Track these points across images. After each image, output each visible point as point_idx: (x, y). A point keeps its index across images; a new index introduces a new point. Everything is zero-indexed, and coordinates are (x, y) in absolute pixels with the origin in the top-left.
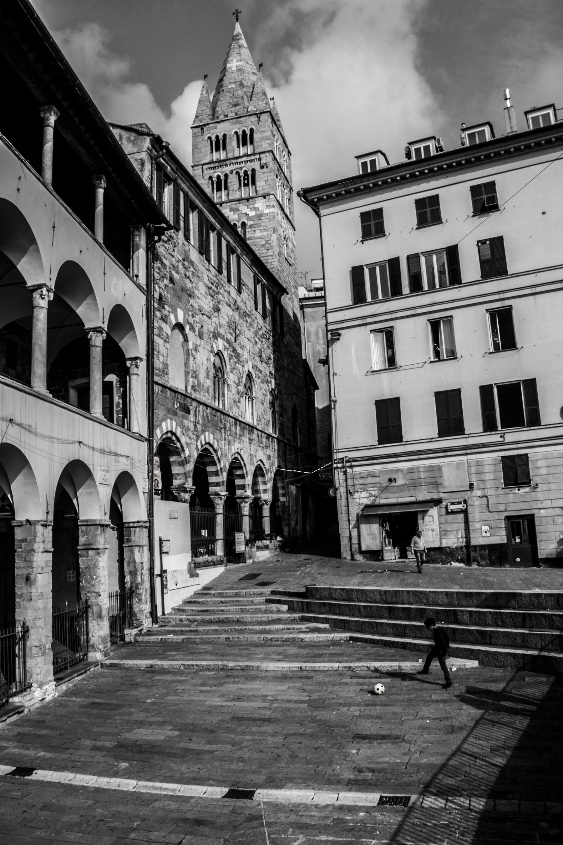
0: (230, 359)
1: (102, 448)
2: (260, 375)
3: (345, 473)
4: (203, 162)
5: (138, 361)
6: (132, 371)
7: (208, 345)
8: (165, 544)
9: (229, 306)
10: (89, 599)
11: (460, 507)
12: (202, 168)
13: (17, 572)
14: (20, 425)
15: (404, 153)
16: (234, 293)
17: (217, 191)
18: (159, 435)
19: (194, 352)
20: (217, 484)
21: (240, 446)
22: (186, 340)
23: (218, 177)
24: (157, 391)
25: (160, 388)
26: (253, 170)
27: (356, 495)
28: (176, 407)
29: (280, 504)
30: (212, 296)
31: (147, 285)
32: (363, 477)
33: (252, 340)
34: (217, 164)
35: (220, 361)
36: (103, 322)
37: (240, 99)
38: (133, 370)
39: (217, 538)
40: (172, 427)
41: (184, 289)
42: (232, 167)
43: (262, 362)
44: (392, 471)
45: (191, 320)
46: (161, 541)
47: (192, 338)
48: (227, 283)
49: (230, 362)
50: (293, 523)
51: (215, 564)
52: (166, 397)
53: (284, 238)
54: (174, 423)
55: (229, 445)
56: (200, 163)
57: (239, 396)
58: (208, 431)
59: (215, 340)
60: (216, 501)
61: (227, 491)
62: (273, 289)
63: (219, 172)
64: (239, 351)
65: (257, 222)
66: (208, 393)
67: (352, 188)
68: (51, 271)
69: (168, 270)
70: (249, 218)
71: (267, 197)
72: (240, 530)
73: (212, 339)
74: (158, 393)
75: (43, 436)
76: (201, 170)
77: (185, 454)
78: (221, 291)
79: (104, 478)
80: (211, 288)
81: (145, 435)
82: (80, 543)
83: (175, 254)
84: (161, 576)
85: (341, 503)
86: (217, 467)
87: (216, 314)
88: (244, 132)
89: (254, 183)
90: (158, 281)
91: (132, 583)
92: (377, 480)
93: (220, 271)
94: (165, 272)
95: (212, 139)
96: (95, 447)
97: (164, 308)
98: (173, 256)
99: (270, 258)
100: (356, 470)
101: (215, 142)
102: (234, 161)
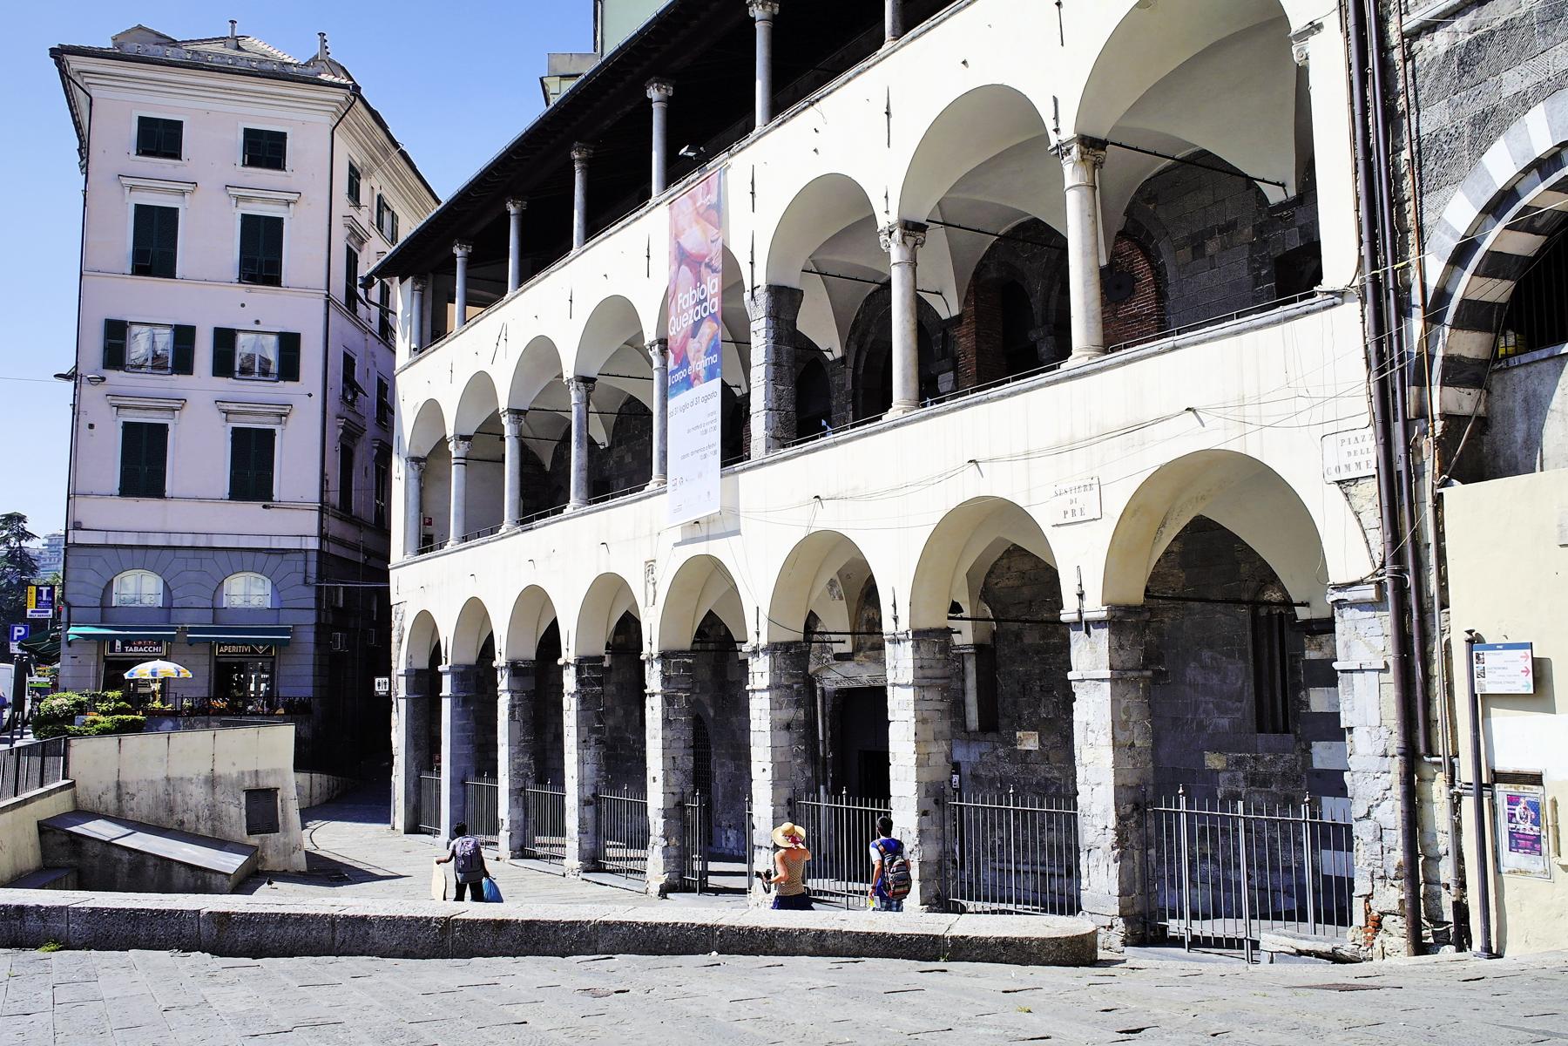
8: (1490, 658)
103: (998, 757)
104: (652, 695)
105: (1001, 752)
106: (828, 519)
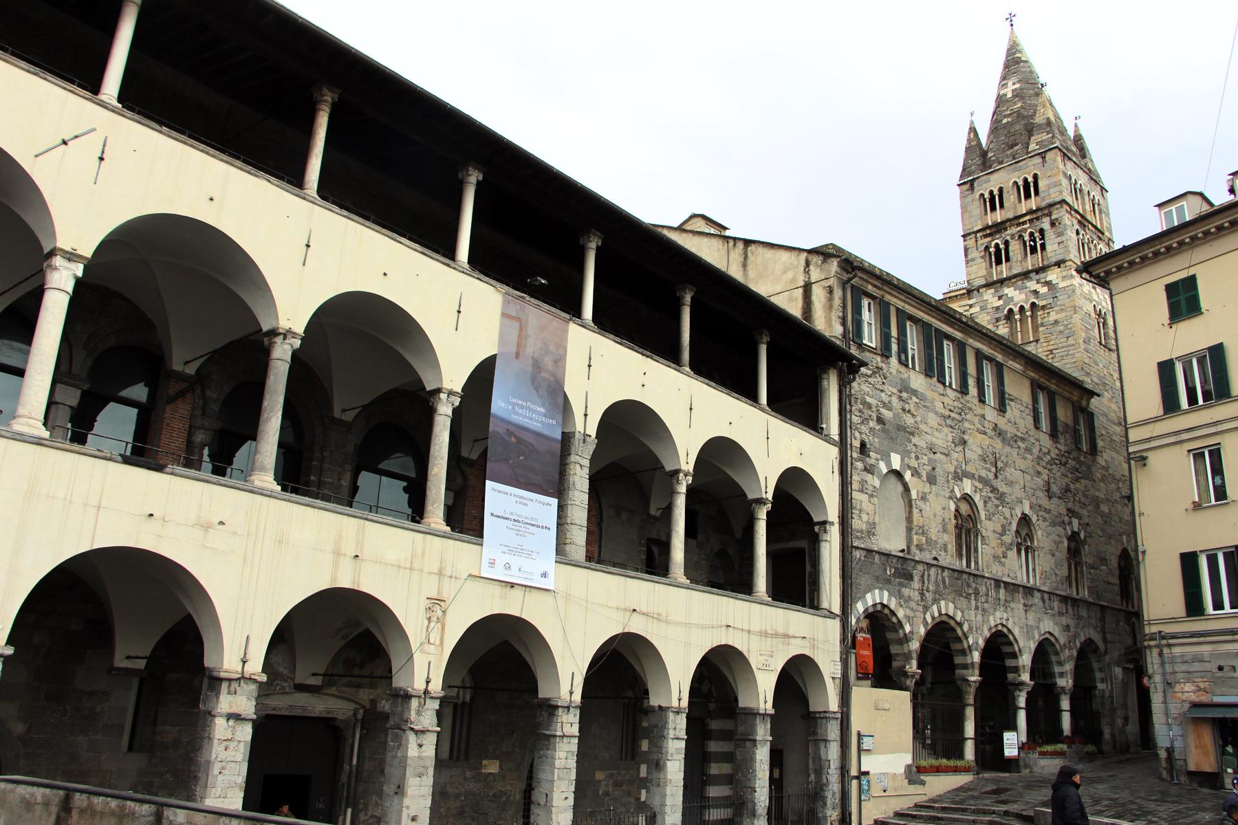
0: (985, 502)
1: (764, 629)
2: (1047, 516)
3: (1161, 654)
4: (975, 229)
6: (821, 538)
7: (944, 490)
8: (865, 739)
9: (985, 433)
10: (744, 794)
12: (976, 237)
14: (644, 614)
15: (1226, 188)
16: (991, 414)
17: (997, 264)
20: (965, 667)
21: (1005, 616)
22: (906, 489)
23: (997, 246)
24: (858, 556)
25: (863, 553)
27: (1177, 688)
28: (888, 573)
29: (1097, 693)
30: (951, 427)
31: (842, 433)
32: (1186, 662)
33: (1031, 471)
34: (994, 229)
35: (969, 507)
36: (766, 493)
40: (881, 597)
41: (901, 428)
42: (1014, 230)
43: (1050, 498)
44: (1228, 655)
45: (914, 463)
46: (859, 735)
47: (916, 487)
48: (977, 404)
49: (985, 506)
50: (1119, 722)
51: (956, 770)
52: (873, 563)
53: (1099, 315)
54: (886, 593)
55: (982, 615)
56: (971, 231)
57: (1004, 550)
59: (959, 483)
60: (964, 689)
61: (979, 676)
62: (1071, 393)
64: (1003, 488)
65: (1051, 301)
66: (946, 551)
67: (1149, 252)
68: (688, 455)
69: (874, 409)
71: (1062, 265)
72: (1013, 727)
73: (952, 481)
74: (860, 559)
75: (676, 624)
76: (974, 240)
77: (904, 630)
78: (968, 417)
79: (765, 663)
80: (950, 416)
83: (885, 387)
84: (857, 778)
85: (1156, 700)
86: (963, 645)
87: (960, 448)
88: (1026, 180)
90: (858, 426)
91: (816, 783)
92: (1208, 666)
93: (964, 390)
94: (870, 413)
95: (986, 197)
96: (752, 630)
97: (869, 456)
98: (882, 391)
99: (1073, 347)
100: (1177, 650)
101: (990, 199)
103: (465, 779)
104: (423, 732)
105: (468, 774)
106: (637, 626)
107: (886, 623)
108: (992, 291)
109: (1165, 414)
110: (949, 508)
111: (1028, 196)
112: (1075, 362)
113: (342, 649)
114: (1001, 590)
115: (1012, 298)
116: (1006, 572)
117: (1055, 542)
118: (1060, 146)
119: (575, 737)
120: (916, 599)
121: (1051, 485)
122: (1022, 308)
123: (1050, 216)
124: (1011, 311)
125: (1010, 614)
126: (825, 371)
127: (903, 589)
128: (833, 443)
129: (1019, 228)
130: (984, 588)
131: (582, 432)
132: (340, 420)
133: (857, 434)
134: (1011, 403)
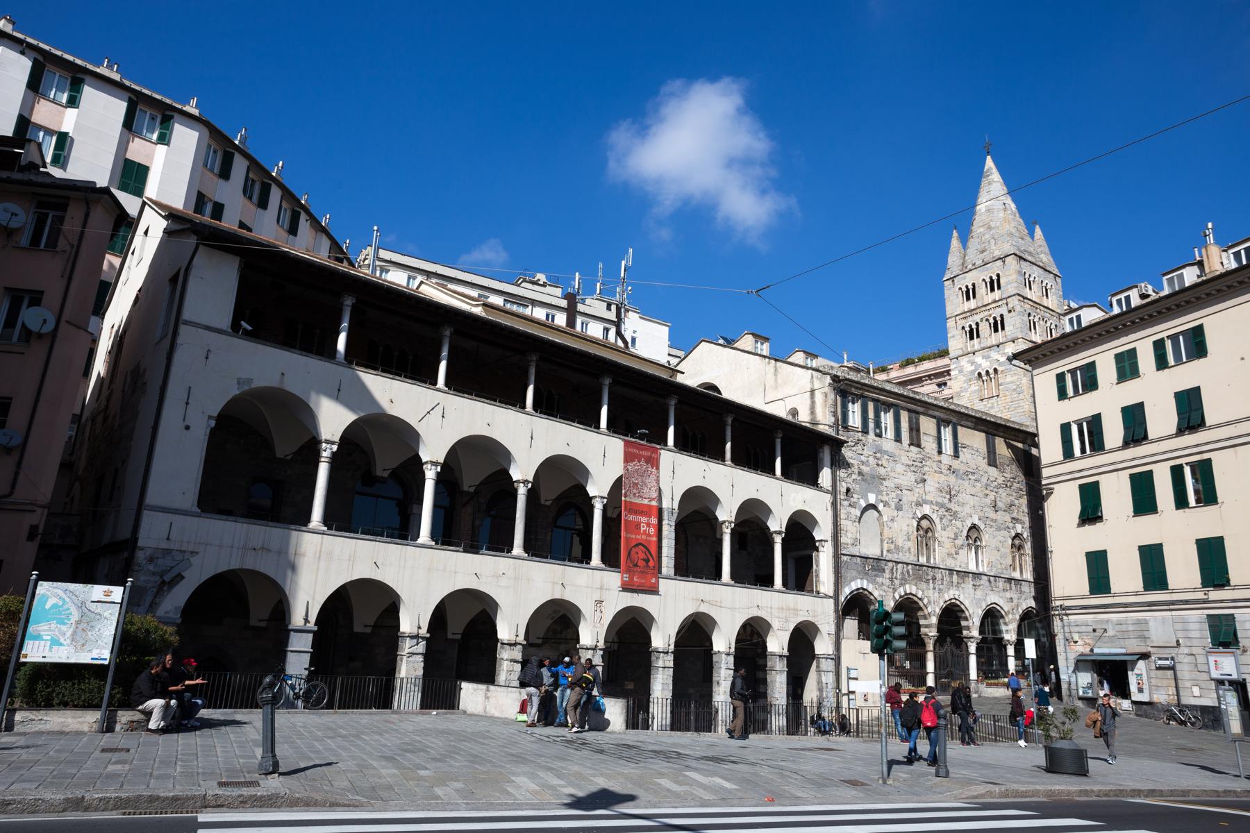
0: (941, 519)
2: (993, 524)
3: (1062, 620)
5: (823, 543)
8: (851, 671)
9: (941, 473)
11: (1167, 663)
13: (714, 678)
16: (946, 459)
17: (970, 340)
18: (848, 592)
19: (888, 523)
20: (927, 626)
21: (957, 593)
23: (970, 326)
26: (1002, 316)
30: (914, 472)
33: (980, 494)
34: (968, 314)
37: (987, 244)
38: (821, 549)
39: (928, 671)
40: (862, 584)
45: (885, 498)
47: (887, 513)
49: (941, 521)
54: (865, 581)
58: (908, 584)
59: (920, 508)
63: (971, 321)
69: (856, 467)
70: (1001, 364)
71: (1016, 341)
76: (954, 322)
78: (928, 463)
81: (832, 594)
82: (768, 666)
83: (864, 452)
87: (921, 485)
88: (991, 278)
89: (1003, 328)
97: (852, 497)
99: (1022, 401)
102: (984, 309)
106: (704, 609)
107: (867, 599)
108: (967, 359)
109: (1064, 460)
110: (912, 525)
111: (992, 290)
112: (1024, 412)
113: (552, 624)
114: (954, 576)
115: (980, 365)
116: (958, 564)
117: (1000, 542)
118: (1018, 253)
119: (671, 668)
120: (888, 584)
121: (997, 502)
122: (987, 372)
123: (1007, 305)
124: (980, 374)
125: (962, 591)
126: (822, 447)
127: (878, 579)
128: (827, 492)
129: (987, 313)
130: (940, 575)
131: (671, 507)
132: (544, 505)
133: (843, 484)
134: (963, 449)
